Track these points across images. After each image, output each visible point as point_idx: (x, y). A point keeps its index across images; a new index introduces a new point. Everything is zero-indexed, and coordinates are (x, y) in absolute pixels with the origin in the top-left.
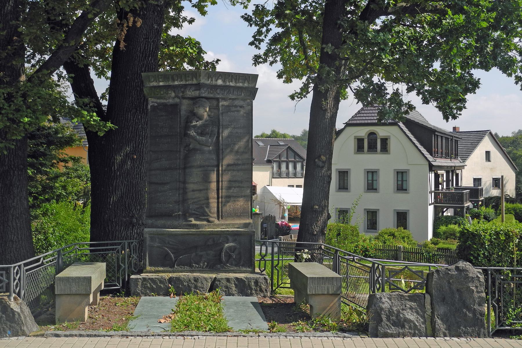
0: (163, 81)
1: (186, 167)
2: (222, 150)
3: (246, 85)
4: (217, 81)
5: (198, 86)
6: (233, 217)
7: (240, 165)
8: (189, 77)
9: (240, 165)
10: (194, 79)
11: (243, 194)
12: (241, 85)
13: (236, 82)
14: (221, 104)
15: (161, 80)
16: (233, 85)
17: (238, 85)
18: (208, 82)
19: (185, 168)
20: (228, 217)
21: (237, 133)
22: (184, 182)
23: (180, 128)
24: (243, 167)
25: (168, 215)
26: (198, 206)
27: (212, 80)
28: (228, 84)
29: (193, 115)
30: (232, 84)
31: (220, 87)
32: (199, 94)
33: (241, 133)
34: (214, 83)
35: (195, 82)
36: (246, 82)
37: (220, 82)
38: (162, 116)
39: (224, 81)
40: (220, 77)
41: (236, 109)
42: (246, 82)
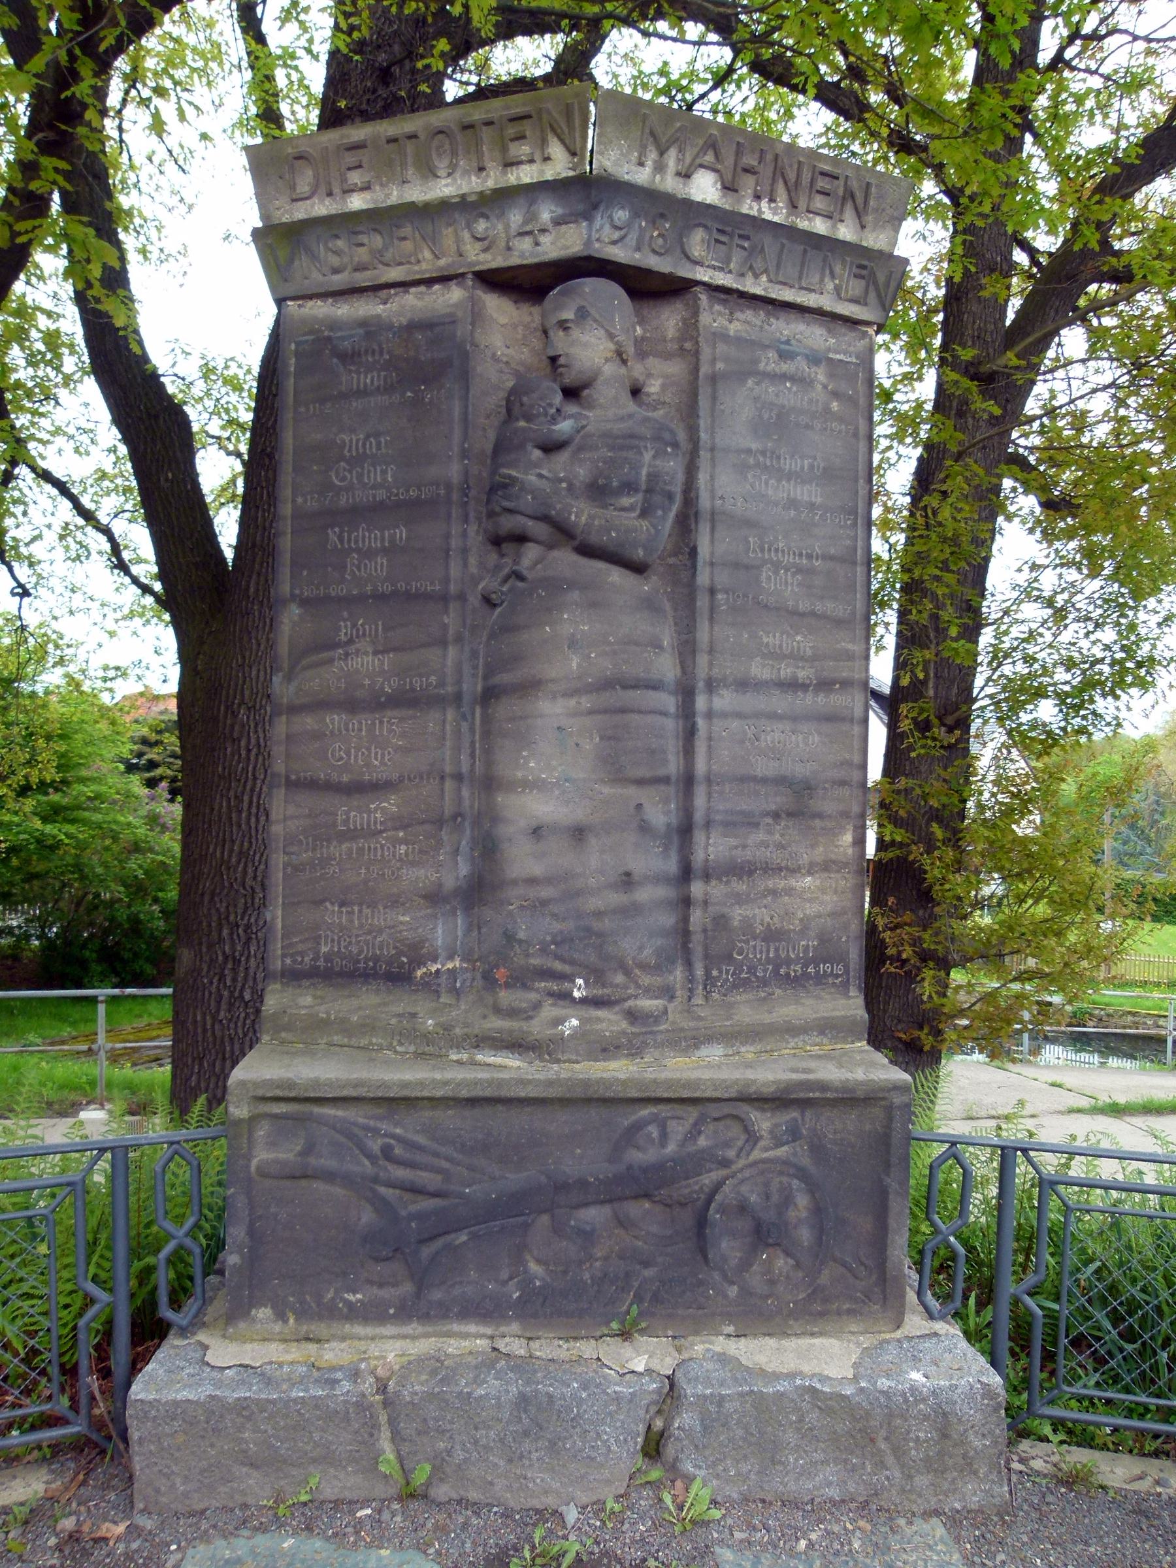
0: (367, 188)
1: (497, 692)
2: (712, 591)
3: (846, 232)
4: (686, 175)
5: (587, 191)
6: (764, 983)
7: (804, 687)
8: (521, 137)
9: (804, 687)
10: (556, 150)
12: (820, 226)
13: (793, 205)
14: (705, 319)
15: (355, 178)
16: (776, 219)
17: (803, 224)
18: (642, 176)
19: (490, 695)
20: (735, 986)
21: (792, 503)
22: (489, 784)
23: (464, 454)
24: (821, 699)
25: (396, 973)
26: (569, 926)
27: (660, 168)
28: (748, 207)
32: (588, 243)
33: (812, 506)
34: (669, 183)
35: (559, 166)
36: (849, 213)
37: (705, 188)
38: (362, 393)
39: (729, 188)
40: (709, 158)
41: (785, 367)
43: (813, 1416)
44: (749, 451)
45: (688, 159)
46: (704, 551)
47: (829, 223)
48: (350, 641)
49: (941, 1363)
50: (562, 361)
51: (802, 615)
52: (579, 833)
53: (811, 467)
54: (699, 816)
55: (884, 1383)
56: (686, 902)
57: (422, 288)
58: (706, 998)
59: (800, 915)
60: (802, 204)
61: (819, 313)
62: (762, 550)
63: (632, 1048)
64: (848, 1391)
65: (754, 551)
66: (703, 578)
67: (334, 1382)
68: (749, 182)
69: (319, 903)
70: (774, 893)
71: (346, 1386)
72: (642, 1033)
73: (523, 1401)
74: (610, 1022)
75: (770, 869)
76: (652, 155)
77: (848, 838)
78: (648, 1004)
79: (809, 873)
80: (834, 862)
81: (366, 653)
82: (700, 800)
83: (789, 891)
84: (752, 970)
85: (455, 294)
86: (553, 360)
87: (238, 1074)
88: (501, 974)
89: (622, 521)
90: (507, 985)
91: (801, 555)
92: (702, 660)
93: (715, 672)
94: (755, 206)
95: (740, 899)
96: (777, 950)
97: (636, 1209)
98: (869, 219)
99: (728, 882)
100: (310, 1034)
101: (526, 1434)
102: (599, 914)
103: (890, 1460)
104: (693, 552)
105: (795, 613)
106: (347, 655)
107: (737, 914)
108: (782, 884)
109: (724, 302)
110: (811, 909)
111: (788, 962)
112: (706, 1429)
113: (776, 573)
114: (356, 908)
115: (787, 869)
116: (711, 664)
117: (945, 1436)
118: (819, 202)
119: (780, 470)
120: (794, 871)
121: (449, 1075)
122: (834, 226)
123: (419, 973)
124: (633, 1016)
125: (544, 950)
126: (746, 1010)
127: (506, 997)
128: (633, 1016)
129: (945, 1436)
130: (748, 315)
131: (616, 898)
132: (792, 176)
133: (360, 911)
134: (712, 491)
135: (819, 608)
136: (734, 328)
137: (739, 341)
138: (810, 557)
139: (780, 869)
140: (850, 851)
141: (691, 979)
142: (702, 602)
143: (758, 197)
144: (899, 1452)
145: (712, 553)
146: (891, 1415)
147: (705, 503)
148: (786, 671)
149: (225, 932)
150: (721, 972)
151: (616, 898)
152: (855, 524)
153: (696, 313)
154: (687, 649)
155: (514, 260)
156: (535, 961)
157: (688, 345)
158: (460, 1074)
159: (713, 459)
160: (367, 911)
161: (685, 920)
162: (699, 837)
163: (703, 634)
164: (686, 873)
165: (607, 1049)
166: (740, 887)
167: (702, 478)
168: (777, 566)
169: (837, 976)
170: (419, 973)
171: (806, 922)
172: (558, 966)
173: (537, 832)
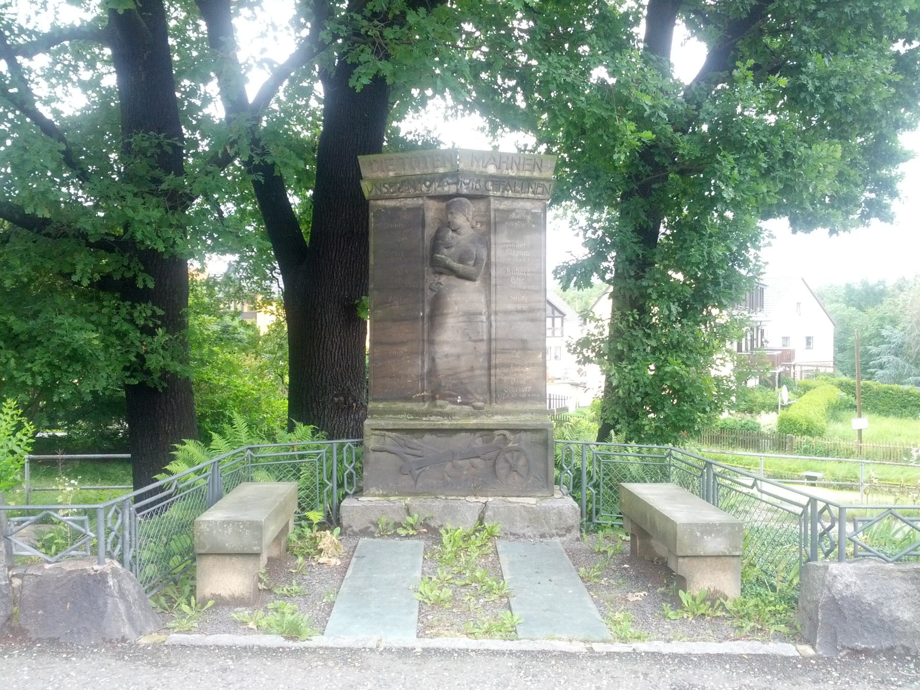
2: (496, 285)
12: (527, 174)
13: (518, 169)
14: (492, 206)
15: (391, 167)
17: (522, 174)
21: (521, 257)
28: (505, 172)
30: (512, 173)
33: (527, 257)
36: (536, 168)
39: (498, 168)
42: (536, 168)
46: (493, 273)
49: (563, 504)
52: (459, 356)
56: (490, 375)
60: (521, 168)
63: (476, 416)
66: (493, 282)
70: (517, 372)
72: (478, 411)
73: (445, 507)
74: (467, 408)
75: (515, 365)
77: (540, 356)
78: (480, 404)
82: (493, 344)
83: (522, 372)
84: (510, 395)
85: (421, 201)
87: (367, 422)
88: (437, 396)
89: (469, 268)
92: (493, 305)
95: (506, 374)
97: (477, 461)
100: (382, 413)
104: (490, 274)
105: (522, 290)
111: (522, 393)
117: (560, 519)
124: (474, 407)
125: (449, 390)
126: (508, 406)
127: (439, 402)
128: (474, 407)
129: (560, 519)
130: (506, 202)
131: (469, 374)
136: (502, 207)
137: (503, 210)
141: (491, 397)
142: (493, 289)
144: (548, 523)
147: (493, 259)
148: (519, 307)
149: (314, 405)
151: (469, 374)
154: (488, 303)
162: (493, 356)
163: (493, 299)
164: (489, 368)
165: (468, 415)
166: (506, 371)
167: (492, 253)
172: (453, 393)
173: (446, 356)
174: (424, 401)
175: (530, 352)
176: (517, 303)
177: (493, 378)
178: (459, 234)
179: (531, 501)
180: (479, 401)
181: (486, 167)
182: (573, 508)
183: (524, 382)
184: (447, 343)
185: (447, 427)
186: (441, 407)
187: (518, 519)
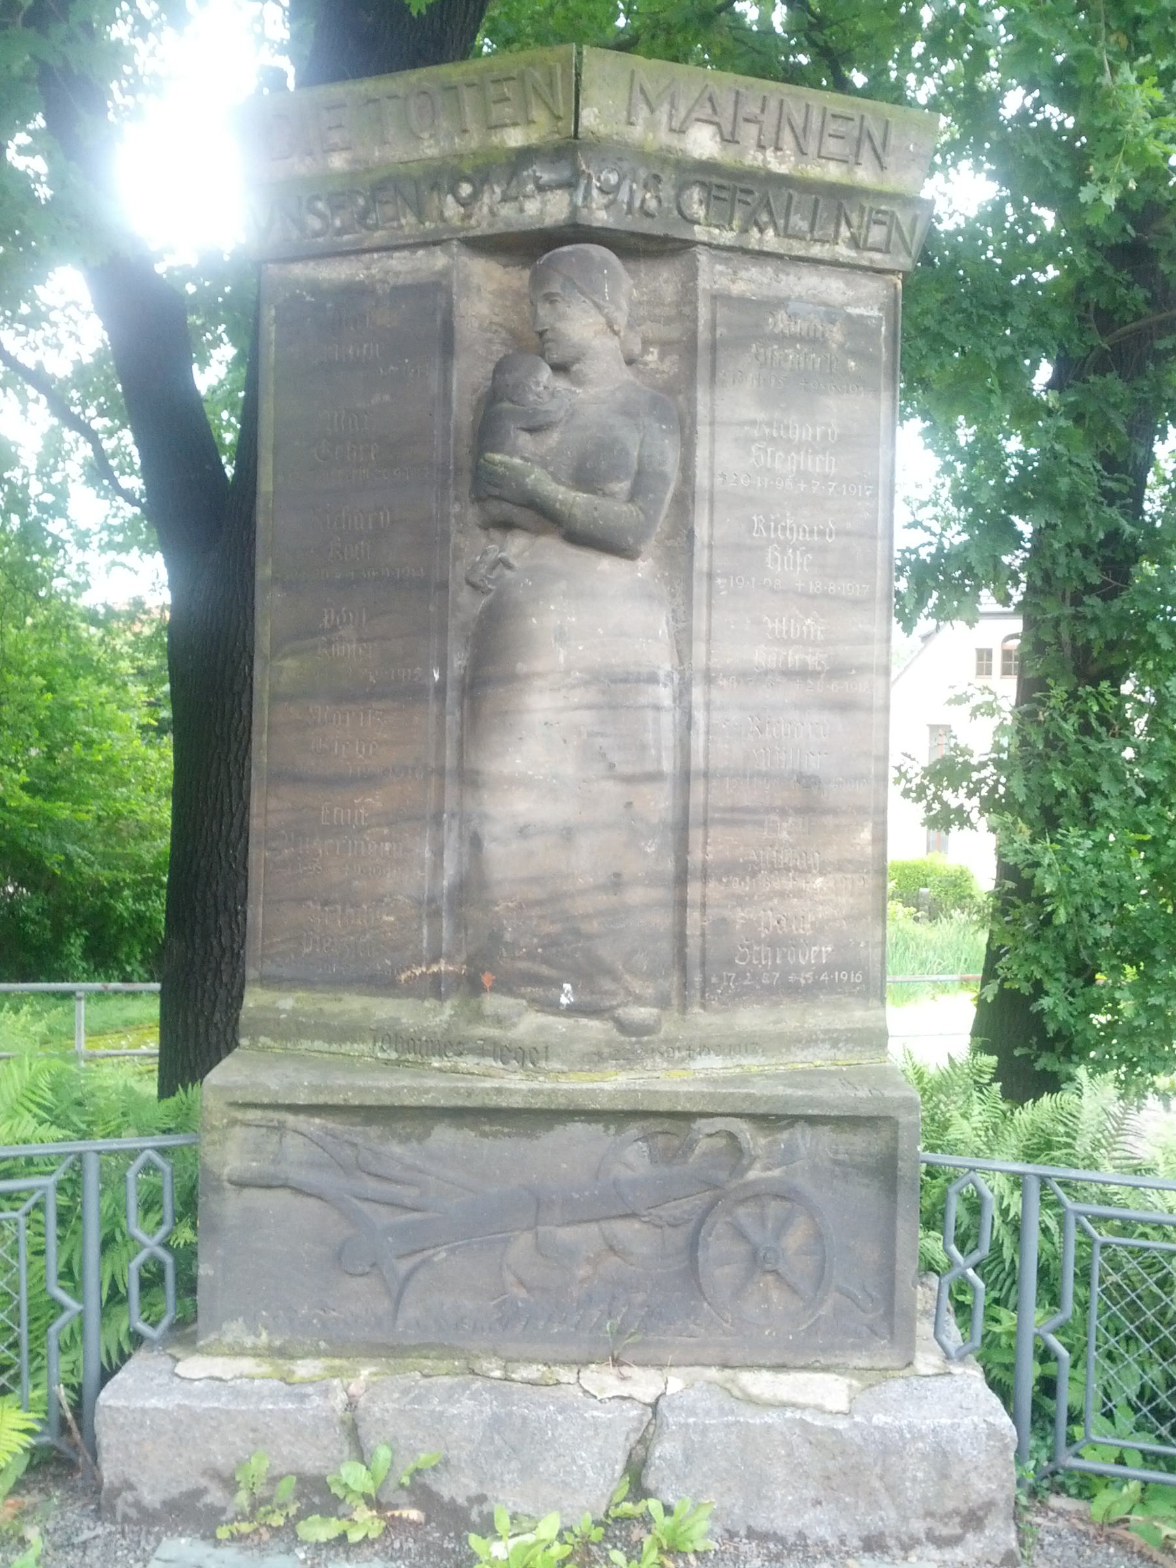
2: (710, 576)
6: (770, 990)
7: (815, 674)
9: (815, 674)
11: (831, 854)
12: (833, 172)
14: (703, 282)
21: (803, 475)
28: (753, 158)
29: (535, 344)
30: (778, 164)
31: (708, 167)
33: (826, 478)
36: (866, 153)
39: (729, 139)
42: (866, 153)
43: (804, 1451)
44: (753, 423)
45: (682, 112)
46: (702, 530)
47: (844, 167)
48: (334, 628)
50: (549, 335)
51: (813, 597)
52: (567, 834)
53: (825, 435)
54: (695, 811)
55: (879, 1419)
56: (682, 904)
57: (406, 253)
58: (703, 1006)
59: (811, 918)
60: (812, 147)
61: (835, 264)
62: (768, 529)
63: (626, 1057)
64: (842, 1424)
65: (759, 531)
66: (701, 562)
67: (303, 1398)
68: (752, 130)
69: (300, 901)
70: (782, 894)
71: (317, 1400)
72: (634, 1043)
73: (496, 1424)
74: (595, 1029)
75: (775, 869)
76: (643, 112)
77: (866, 835)
78: (641, 1013)
79: (822, 873)
80: (850, 862)
81: (350, 641)
83: (799, 893)
84: (756, 976)
85: (439, 260)
86: (541, 334)
88: (487, 979)
89: (613, 507)
90: (493, 989)
91: (812, 532)
92: (699, 649)
93: (716, 663)
94: (760, 157)
95: (740, 901)
96: (784, 956)
97: (625, 1230)
98: (888, 160)
99: (728, 884)
101: (498, 1455)
102: (587, 917)
103: (885, 1501)
104: (691, 535)
106: (330, 643)
107: (740, 915)
108: (789, 885)
109: (726, 261)
110: (824, 912)
111: (798, 969)
112: (688, 1459)
113: (783, 552)
114: (339, 907)
115: (796, 869)
116: (709, 654)
118: (832, 146)
119: (789, 441)
120: (802, 872)
121: (430, 1083)
122: (850, 171)
123: (403, 977)
124: (623, 1027)
125: (531, 956)
126: (750, 1018)
127: (493, 1003)
128: (623, 1027)
129: (944, 1476)
130: (754, 272)
132: (799, 121)
133: (343, 910)
134: (712, 470)
135: (832, 588)
137: (742, 302)
138: (822, 533)
139: (788, 870)
140: (869, 850)
141: (685, 985)
142: (700, 589)
143: (761, 147)
145: (711, 536)
146: (885, 1452)
147: (702, 478)
148: (795, 657)
150: (721, 978)
151: (603, 900)
152: (875, 495)
153: (694, 276)
154: (683, 640)
155: (500, 227)
156: (523, 965)
157: (687, 310)
158: (442, 1083)
159: (712, 436)
160: (350, 911)
161: (682, 922)
162: (696, 835)
163: (700, 624)
164: (681, 878)
165: (596, 1058)
166: (740, 887)
167: (701, 454)
168: (784, 546)
169: (855, 985)
170: (403, 977)
171: (819, 928)
172: (545, 970)
173: (523, 832)
174: (439, 996)
175: (829, 820)
176: (787, 642)
177: (694, 917)
178: (579, 381)
179: (825, 1392)
180: (639, 1000)
181: (682, 131)
182: (993, 1432)
183: (806, 930)
184: (523, 782)
185: (517, 1102)
186: (499, 1021)
187: (779, 1472)
